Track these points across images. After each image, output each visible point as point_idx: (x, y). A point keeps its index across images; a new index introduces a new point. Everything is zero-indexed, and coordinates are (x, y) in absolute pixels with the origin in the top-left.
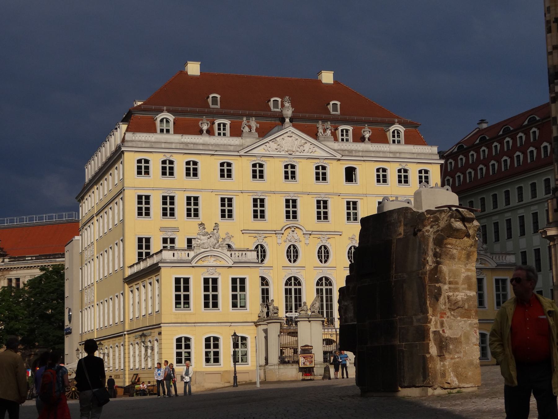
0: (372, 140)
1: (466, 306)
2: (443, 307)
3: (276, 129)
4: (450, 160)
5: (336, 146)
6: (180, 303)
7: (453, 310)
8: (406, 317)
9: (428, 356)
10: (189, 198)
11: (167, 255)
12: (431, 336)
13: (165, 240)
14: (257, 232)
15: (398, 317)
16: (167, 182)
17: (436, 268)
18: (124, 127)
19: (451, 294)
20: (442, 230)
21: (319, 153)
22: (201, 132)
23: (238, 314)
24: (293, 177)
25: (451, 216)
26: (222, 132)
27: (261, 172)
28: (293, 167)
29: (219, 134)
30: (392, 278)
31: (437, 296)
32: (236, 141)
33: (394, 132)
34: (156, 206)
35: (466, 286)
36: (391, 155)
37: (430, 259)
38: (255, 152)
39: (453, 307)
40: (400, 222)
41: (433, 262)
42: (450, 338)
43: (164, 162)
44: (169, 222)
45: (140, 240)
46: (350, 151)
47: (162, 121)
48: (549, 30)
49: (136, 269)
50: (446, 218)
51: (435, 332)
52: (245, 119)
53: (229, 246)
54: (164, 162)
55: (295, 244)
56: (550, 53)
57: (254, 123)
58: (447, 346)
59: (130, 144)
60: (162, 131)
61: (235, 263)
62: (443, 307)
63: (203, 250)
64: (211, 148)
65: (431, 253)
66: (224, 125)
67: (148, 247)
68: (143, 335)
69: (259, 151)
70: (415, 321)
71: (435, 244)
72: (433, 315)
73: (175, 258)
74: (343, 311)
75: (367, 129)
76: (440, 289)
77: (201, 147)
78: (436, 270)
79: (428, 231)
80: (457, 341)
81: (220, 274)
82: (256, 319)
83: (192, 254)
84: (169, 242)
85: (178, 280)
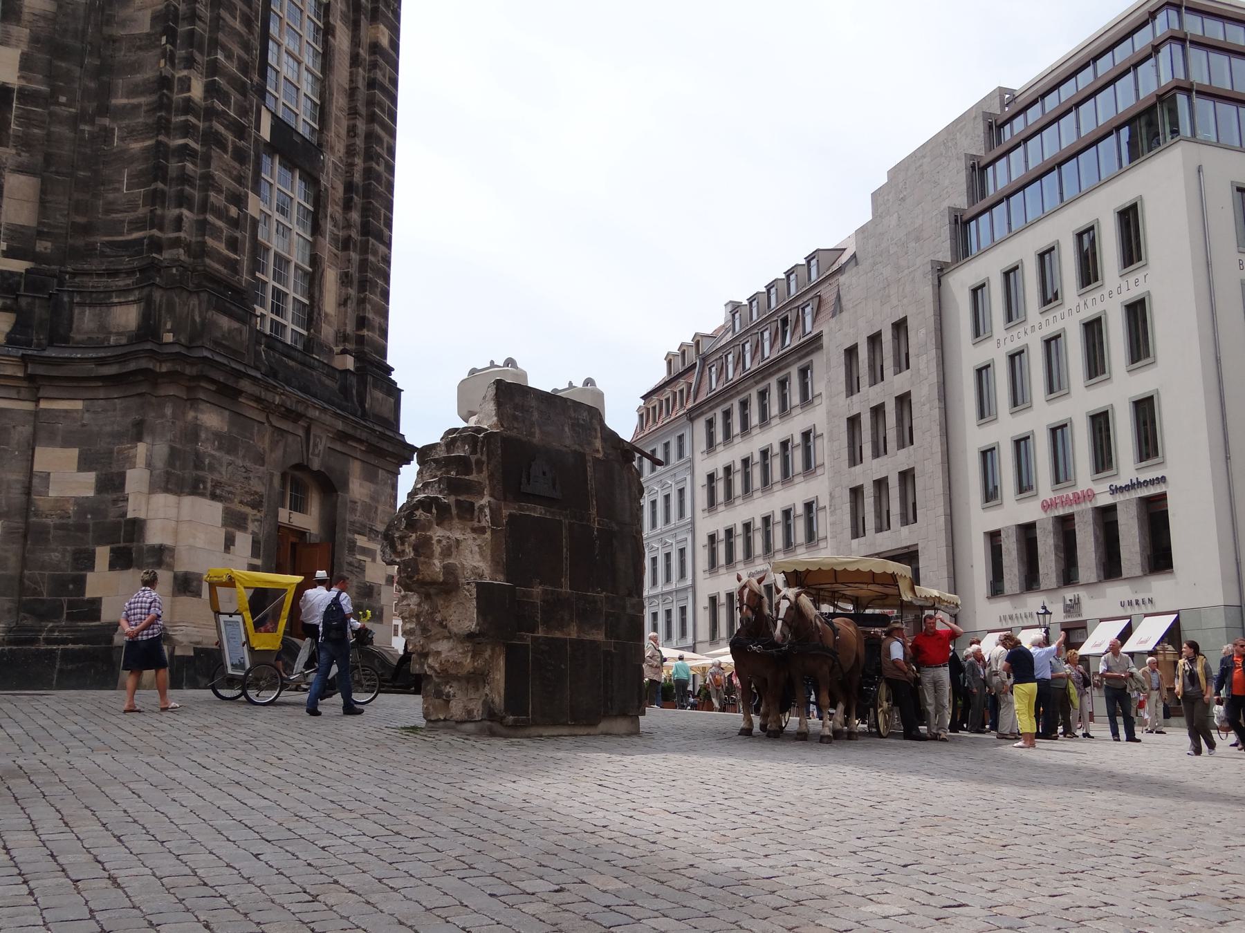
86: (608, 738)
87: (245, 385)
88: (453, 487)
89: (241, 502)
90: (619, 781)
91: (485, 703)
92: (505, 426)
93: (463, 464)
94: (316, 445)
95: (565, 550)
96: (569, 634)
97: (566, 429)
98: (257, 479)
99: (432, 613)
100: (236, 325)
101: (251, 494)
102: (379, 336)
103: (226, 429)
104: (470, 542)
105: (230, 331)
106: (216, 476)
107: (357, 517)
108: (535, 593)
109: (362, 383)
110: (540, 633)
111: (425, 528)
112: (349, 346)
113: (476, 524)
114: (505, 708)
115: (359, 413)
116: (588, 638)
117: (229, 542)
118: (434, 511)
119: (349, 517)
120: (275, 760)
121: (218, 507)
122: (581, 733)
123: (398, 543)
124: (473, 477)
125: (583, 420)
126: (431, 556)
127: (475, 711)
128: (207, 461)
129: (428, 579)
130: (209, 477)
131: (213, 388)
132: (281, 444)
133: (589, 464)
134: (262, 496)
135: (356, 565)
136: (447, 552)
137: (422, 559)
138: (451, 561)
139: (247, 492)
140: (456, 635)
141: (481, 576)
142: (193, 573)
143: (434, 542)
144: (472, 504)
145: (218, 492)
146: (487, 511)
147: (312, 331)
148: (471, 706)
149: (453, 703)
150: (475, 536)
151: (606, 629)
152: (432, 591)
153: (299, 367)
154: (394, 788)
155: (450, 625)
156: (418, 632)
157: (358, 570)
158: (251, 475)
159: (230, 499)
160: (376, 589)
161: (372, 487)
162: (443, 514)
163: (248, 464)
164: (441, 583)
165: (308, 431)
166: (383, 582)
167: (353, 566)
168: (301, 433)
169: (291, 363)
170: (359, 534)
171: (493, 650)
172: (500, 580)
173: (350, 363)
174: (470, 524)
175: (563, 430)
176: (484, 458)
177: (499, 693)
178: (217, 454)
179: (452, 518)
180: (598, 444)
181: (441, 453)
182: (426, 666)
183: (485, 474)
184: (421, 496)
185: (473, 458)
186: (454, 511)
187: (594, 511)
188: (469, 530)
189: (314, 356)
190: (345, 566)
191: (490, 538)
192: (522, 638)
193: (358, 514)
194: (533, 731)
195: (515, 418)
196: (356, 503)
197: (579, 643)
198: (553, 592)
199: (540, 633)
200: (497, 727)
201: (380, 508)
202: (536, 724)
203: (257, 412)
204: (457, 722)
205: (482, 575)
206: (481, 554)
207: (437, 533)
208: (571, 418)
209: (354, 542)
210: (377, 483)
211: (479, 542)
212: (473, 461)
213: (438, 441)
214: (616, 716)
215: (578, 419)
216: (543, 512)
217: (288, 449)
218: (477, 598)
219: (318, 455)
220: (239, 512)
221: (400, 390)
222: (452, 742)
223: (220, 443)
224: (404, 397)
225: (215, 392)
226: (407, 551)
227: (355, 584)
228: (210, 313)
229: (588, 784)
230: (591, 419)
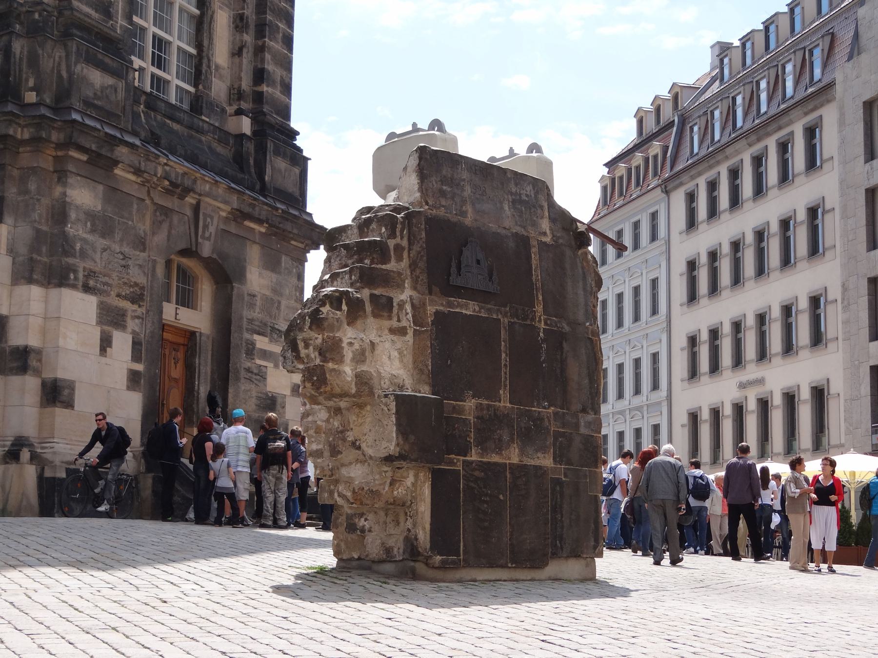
8: (567, 413)
15: (553, 408)
30: (540, 321)
70: (583, 424)
86: (556, 584)
87: (122, 152)
88: (367, 278)
89: (118, 295)
90: (566, 636)
91: (407, 539)
92: (430, 203)
93: (380, 251)
94: (206, 227)
95: (503, 355)
96: (509, 459)
97: (506, 207)
98: (137, 268)
99: (342, 432)
100: (110, 81)
101: (131, 286)
102: (281, 92)
103: (99, 208)
104: (387, 345)
105: (103, 88)
106: (89, 265)
107: (257, 314)
108: (467, 408)
109: (261, 150)
110: (474, 456)
111: (332, 328)
112: (244, 105)
113: (394, 323)
114: (430, 547)
115: (258, 187)
116: (532, 462)
117: (106, 343)
118: (344, 307)
119: (247, 314)
120: (158, 604)
121: (92, 301)
122: (524, 578)
123: (301, 345)
124: (392, 266)
125: (527, 196)
126: (341, 360)
127: (396, 550)
128: (78, 246)
129: (337, 390)
130: (81, 265)
131: (84, 158)
132: (165, 226)
133: (533, 250)
134: (143, 288)
135: (255, 371)
136: (360, 357)
137: (330, 365)
138: (364, 368)
139: (125, 283)
140: (371, 458)
141: (401, 387)
142: (65, 380)
143: (344, 345)
144: (390, 300)
145: (91, 283)
146: (408, 308)
147: (201, 87)
148: (391, 543)
149: (369, 538)
150: (395, 338)
151: (554, 453)
152: (343, 404)
153: (186, 131)
154: (296, 639)
155: (363, 446)
156: (327, 454)
157: (258, 377)
158: (130, 263)
159: (105, 291)
160: (279, 401)
161: (274, 276)
162: (355, 309)
163: (126, 250)
164: (354, 396)
165: (196, 209)
166: (288, 392)
167: (252, 372)
168: (189, 212)
169: (176, 126)
170: (259, 334)
171: (416, 476)
172: (425, 392)
173: (246, 125)
174: (387, 324)
175: (502, 208)
176: (405, 243)
177: (424, 529)
178: (90, 237)
179: (366, 317)
180: (545, 225)
181: (353, 238)
182: (336, 495)
183: (405, 263)
184: (328, 290)
185: (391, 243)
186: (368, 308)
187: (539, 309)
188: (387, 332)
189: (203, 118)
190: (243, 373)
191: (411, 341)
192: (451, 462)
193: (257, 310)
195: (443, 194)
196: (254, 296)
197: (520, 470)
198: (489, 406)
199: (474, 456)
200: (420, 567)
201: (284, 303)
202: (468, 565)
203: (137, 186)
204: (373, 562)
205: (402, 386)
206: (401, 361)
207: (348, 335)
208: (512, 194)
209: (253, 344)
210: (279, 273)
211: (399, 345)
212: (392, 248)
213: (348, 221)
214: (567, 557)
215: (520, 194)
216: (477, 309)
217: (173, 231)
218: (397, 413)
219: (209, 239)
220: (116, 307)
221: (306, 159)
222: (368, 586)
223: (93, 225)
224: (310, 165)
225: (87, 162)
226: (313, 356)
227: (254, 394)
228: (79, 67)
229: (529, 639)
230: (537, 193)
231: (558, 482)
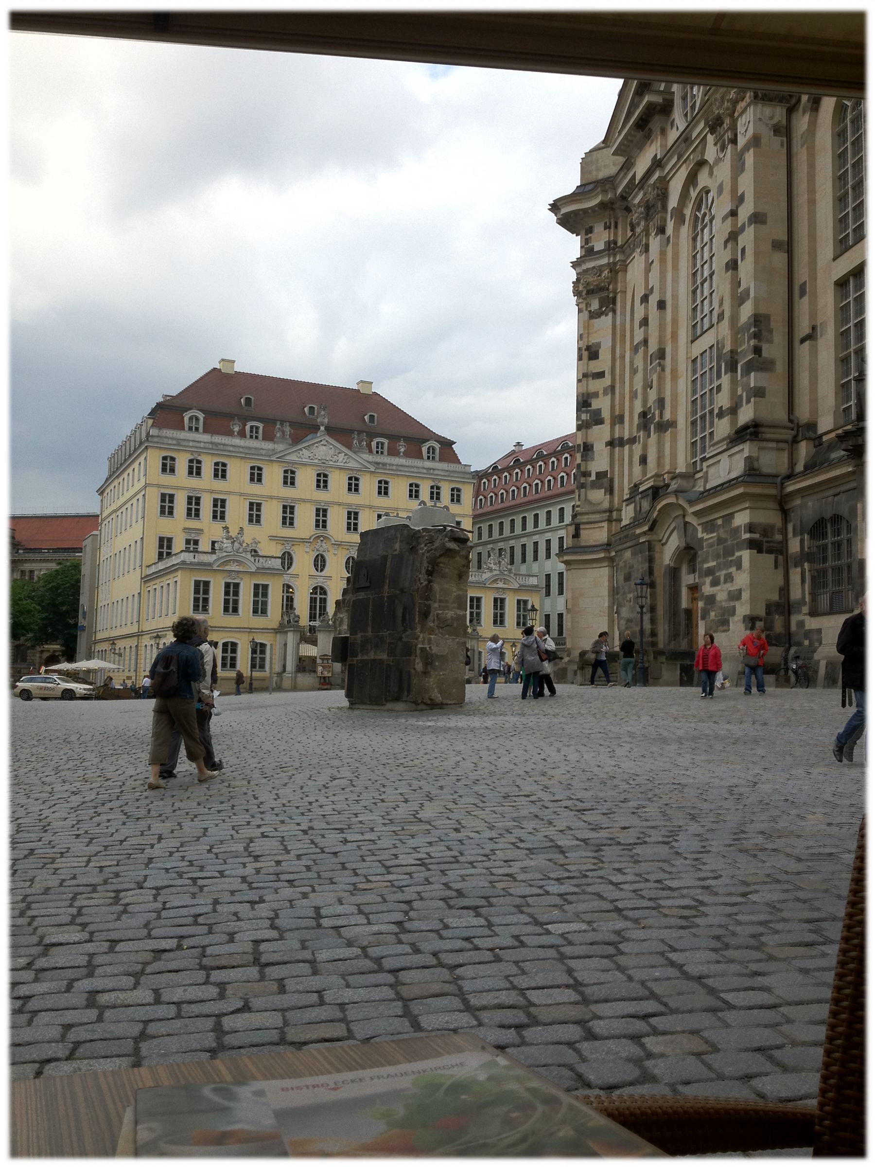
0: (407, 455)
1: (455, 625)
2: (432, 625)
3: (309, 437)
4: (485, 480)
5: (370, 458)
6: (198, 606)
7: (442, 628)
9: (413, 671)
10: (215, 500)
11: (188, 557)
12: (418, 651)
13: (188, 542)
14: (285, 540)
16: (194, 482)
17: (427, 586)
18: (150, 422)
19: (440, 612)
20: (436, 549)
21: (352, 464)
22: (230, 433)
23: (259, 622)
24: (325, 486)
25: (446, 536)
26: (254, 434)
27: (293, 478)
28: (326, 476)
29: (251, 437)
31: (425, 615)
32: (268, 445)
33: (429, 448)
34: (180, 505)
35: (456, 605)
36: (425, 471)
37: (423, 578)
38: (288, 458)
39: (441, 625)
40: (397, 538)
41: (425, 580)
42: (437, 655)
43: (191, 461)
44: (193, 524)
45: (161, 539)
46: (384, 464)
47: (191, 418)
48: (580, 358)
49: (153, 569)
50: (440, 537)
51: (421, 649)
52: (278, 423)
53: (255, 551)
54: (191, 461)
55: (324, 554)
56: (579, 381)
57: (287, 429)
58: (431, 663)
59: (155, 440)
60: (190, 429)
61: (258, 568)
62: (432, 625)
63: (225, 554)
64: (241, 450)
65: (424, 571)
66: (257, 428)
67: (169, 547)
68: (158, 637)
69: (293, 457)
71: (429, 562)
72: (421, 632)
73: (196, 560)
74: (338, 623)
75: (402, 443)
76: (429, 607)
77: (231, 449)
78: (429, 588)
79: (421, 549)
80: (443, 658)
81: (242, 579)
82: (275, 625)
83: (214, 557)
84: (192, 544)
85: (197, 583)
110: (359, 658)
194: (357, 706)
197: (375, 660)
199: (359, 658)
231: (388, 665)
